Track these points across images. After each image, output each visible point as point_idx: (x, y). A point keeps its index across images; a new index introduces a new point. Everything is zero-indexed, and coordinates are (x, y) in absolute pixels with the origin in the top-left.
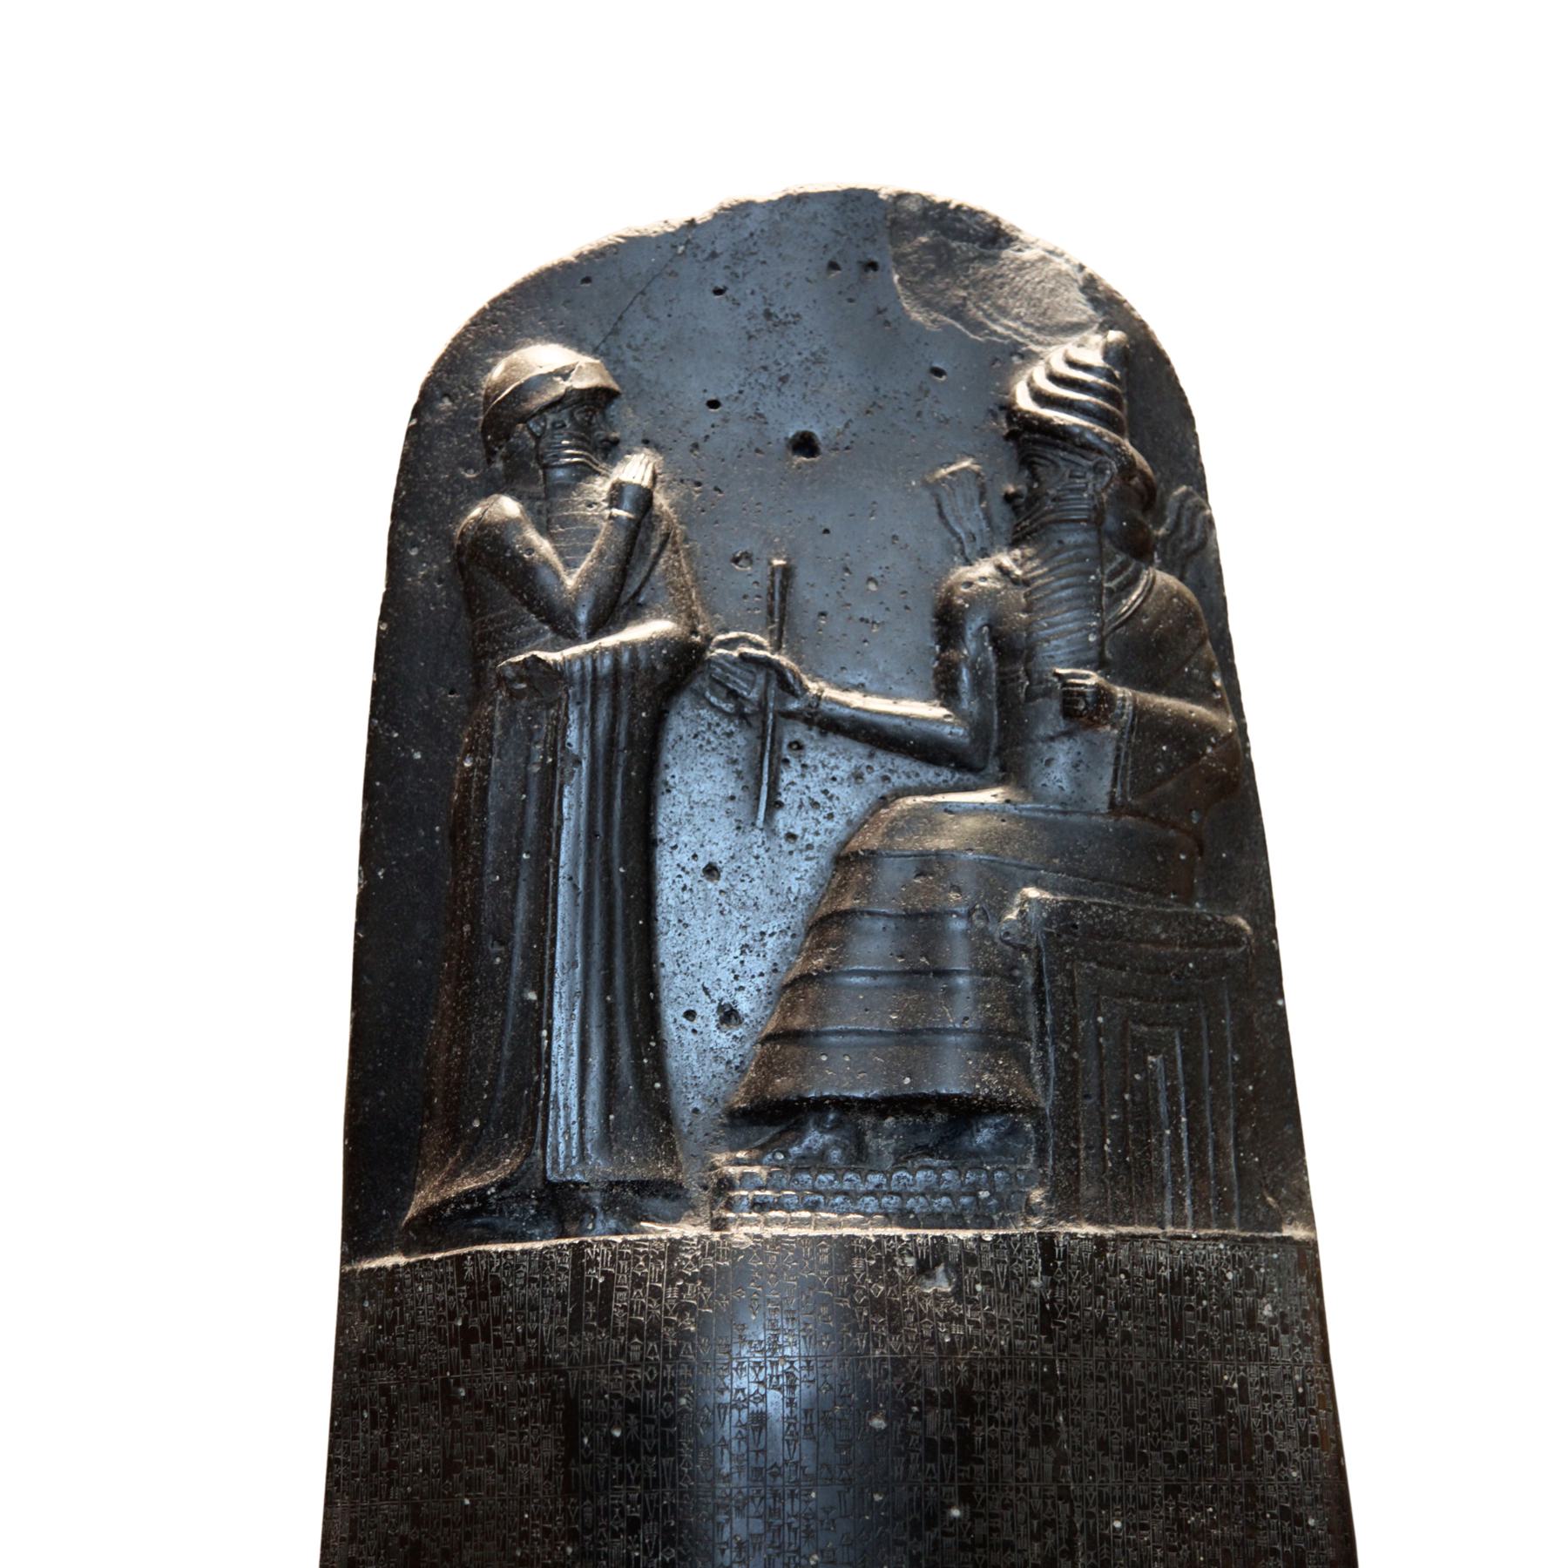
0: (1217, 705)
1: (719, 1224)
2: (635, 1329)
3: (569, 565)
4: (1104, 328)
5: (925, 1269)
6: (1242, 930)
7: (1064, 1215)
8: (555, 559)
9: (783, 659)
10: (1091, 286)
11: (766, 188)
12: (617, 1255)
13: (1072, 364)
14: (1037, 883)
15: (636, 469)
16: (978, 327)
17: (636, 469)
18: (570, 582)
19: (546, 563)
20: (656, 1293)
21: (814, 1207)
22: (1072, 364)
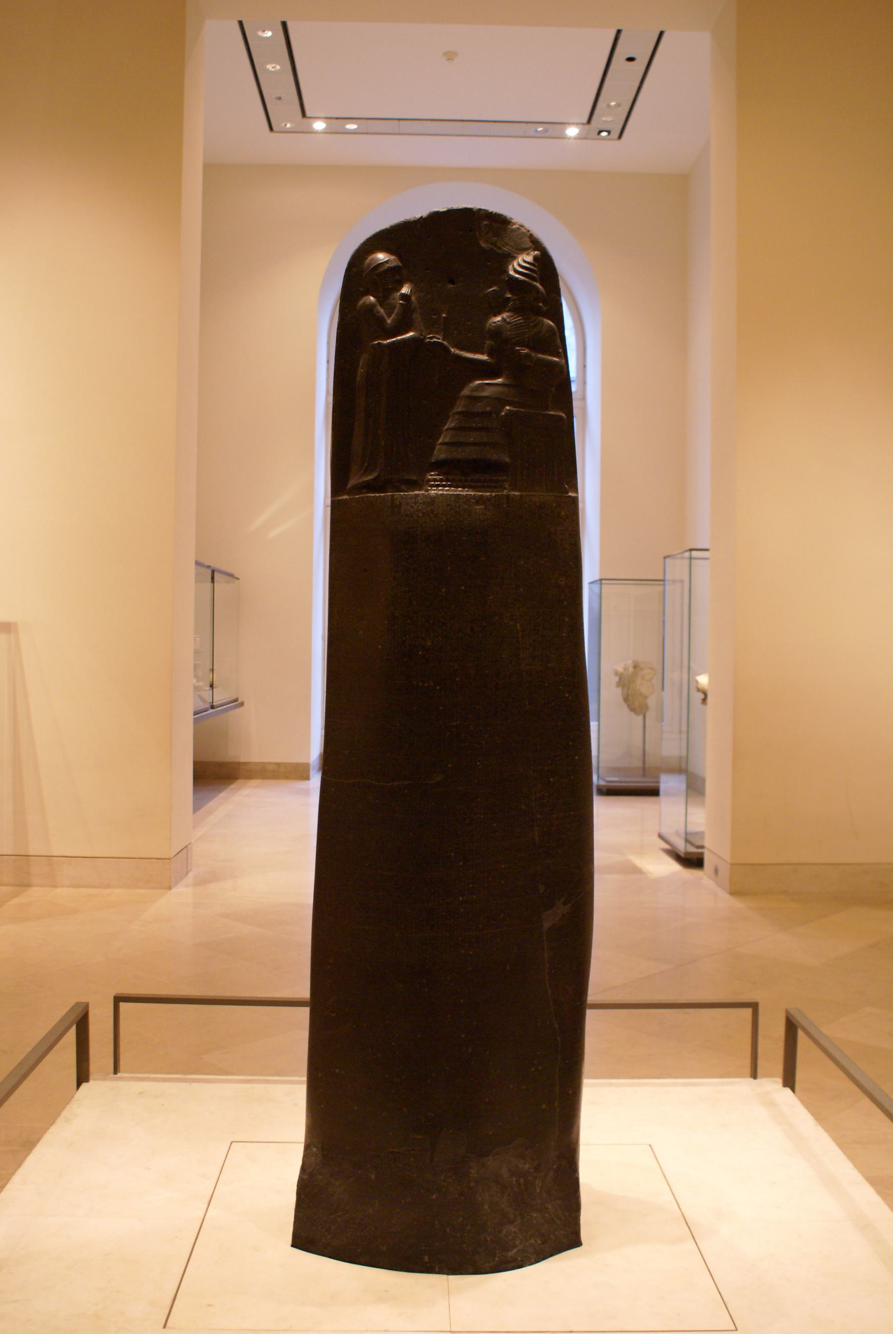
0: (559, 357)
1: (427, 491)
2: (407, 515)
3: (389, 317)
4: (535, 250)
5: (477, 503)
6: (561, 417)
7: (513, 490)
8: (385, 315)
9: (445, 343)
10: (531, 236)
11: (442, 209)
12: (402, 497)
13: (525, 261)
14: (509, 405)
15: (405, 290)
16: (500, 248)
17: (405, 290)
18: (389, 321)
19: (383, 317)
20: (412, 507)
21: (449, 486)
22: (525, 261)
